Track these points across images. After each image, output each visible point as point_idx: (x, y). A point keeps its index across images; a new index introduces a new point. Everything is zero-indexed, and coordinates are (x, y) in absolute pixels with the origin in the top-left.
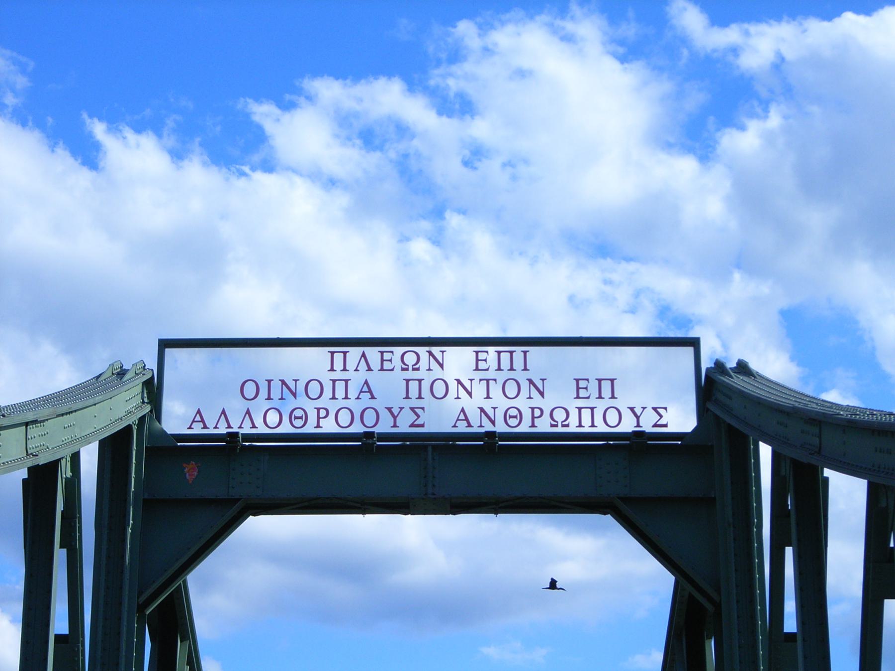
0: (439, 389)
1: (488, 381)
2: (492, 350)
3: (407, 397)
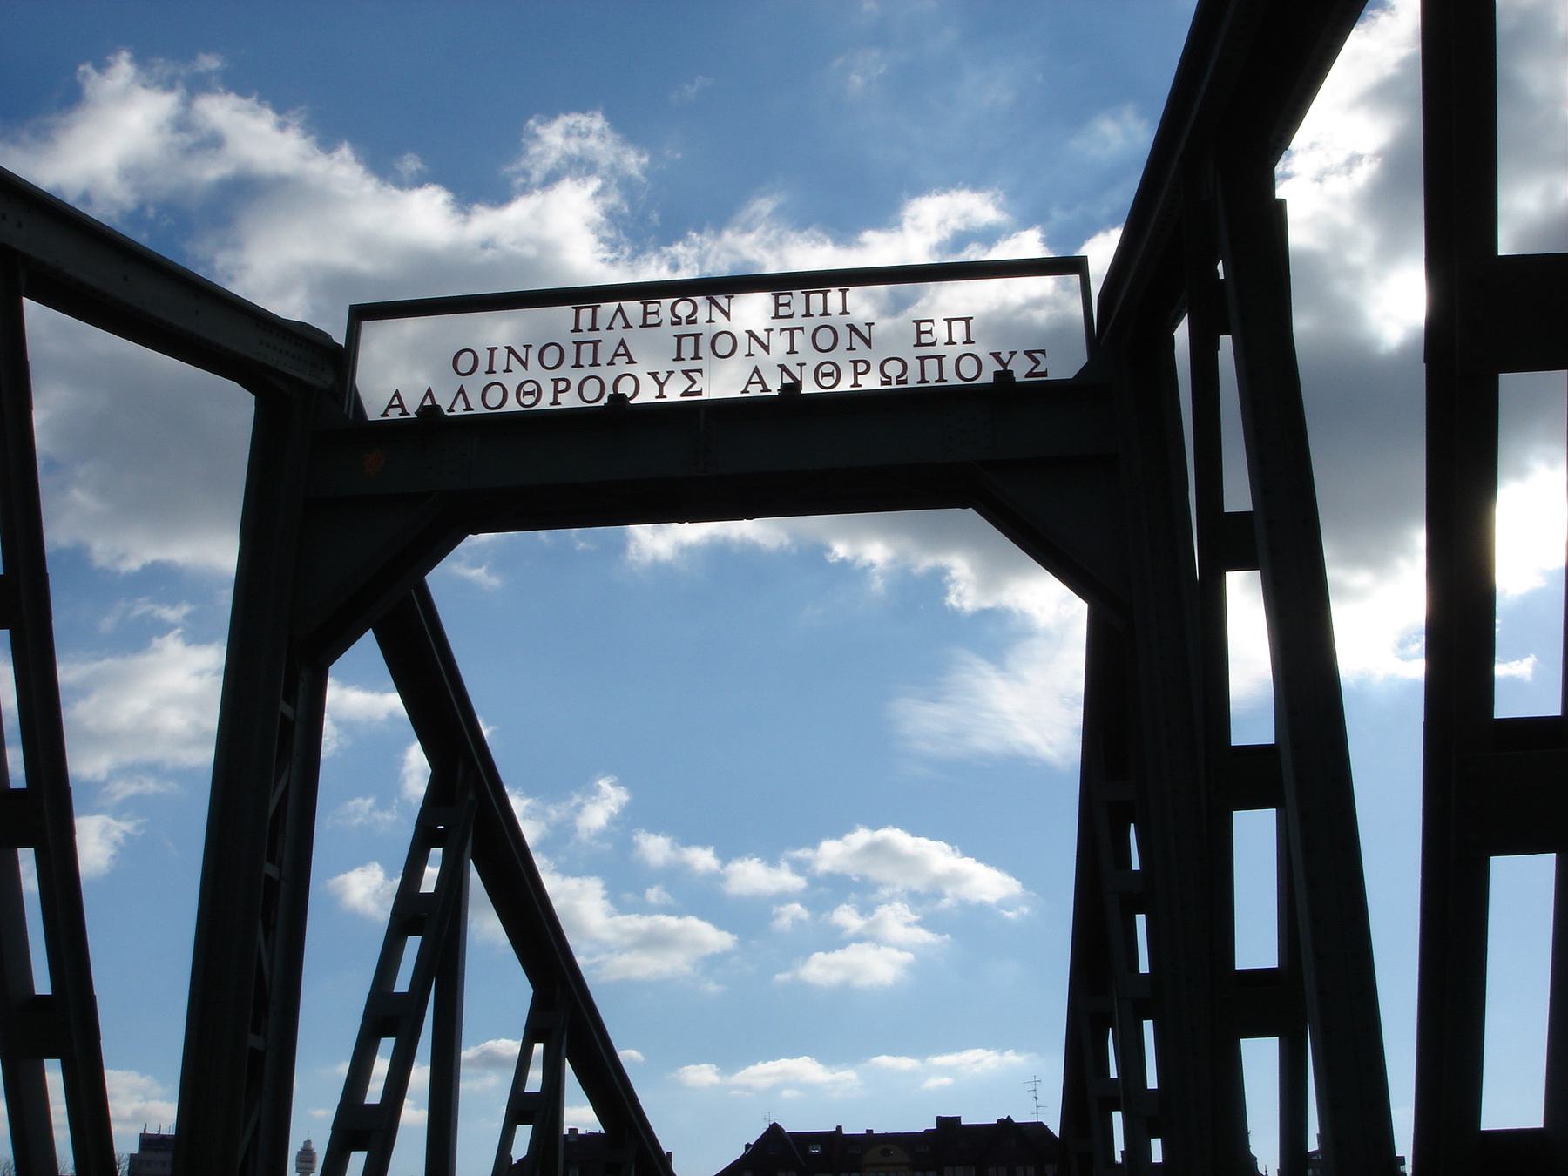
0: (724, 345)
1: (792, 330)
2: (798, 295)
3: (679, 358)
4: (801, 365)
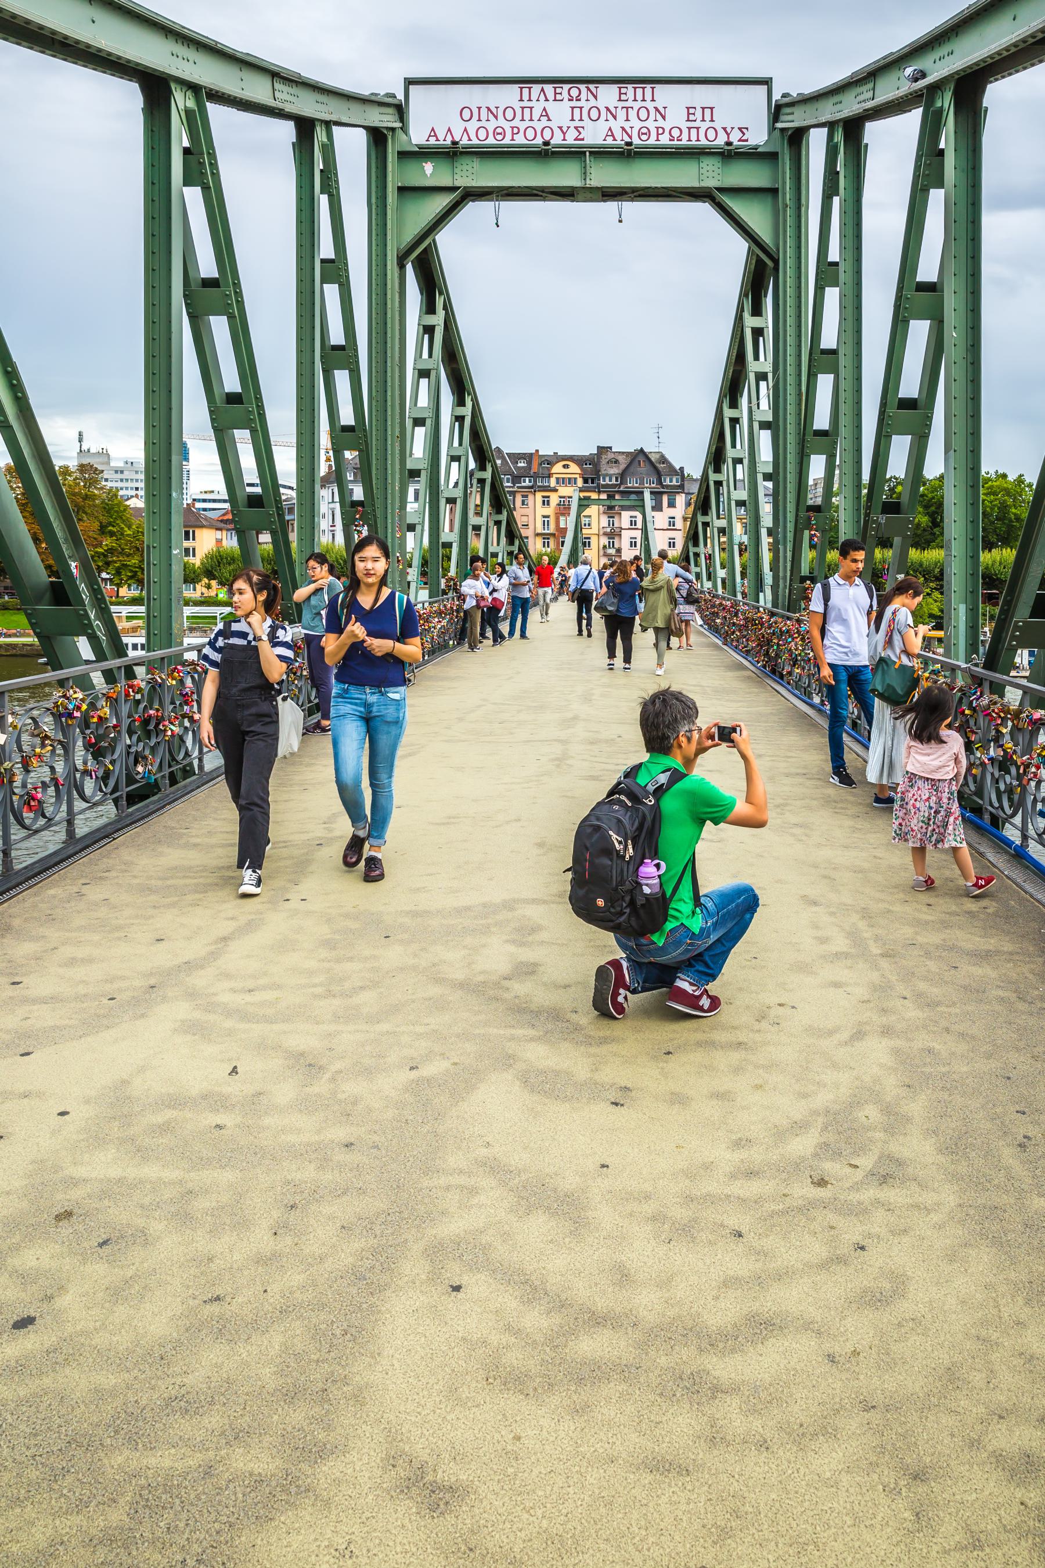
0: (594, 114)
3: (572, 120)
4: (632, 128)
